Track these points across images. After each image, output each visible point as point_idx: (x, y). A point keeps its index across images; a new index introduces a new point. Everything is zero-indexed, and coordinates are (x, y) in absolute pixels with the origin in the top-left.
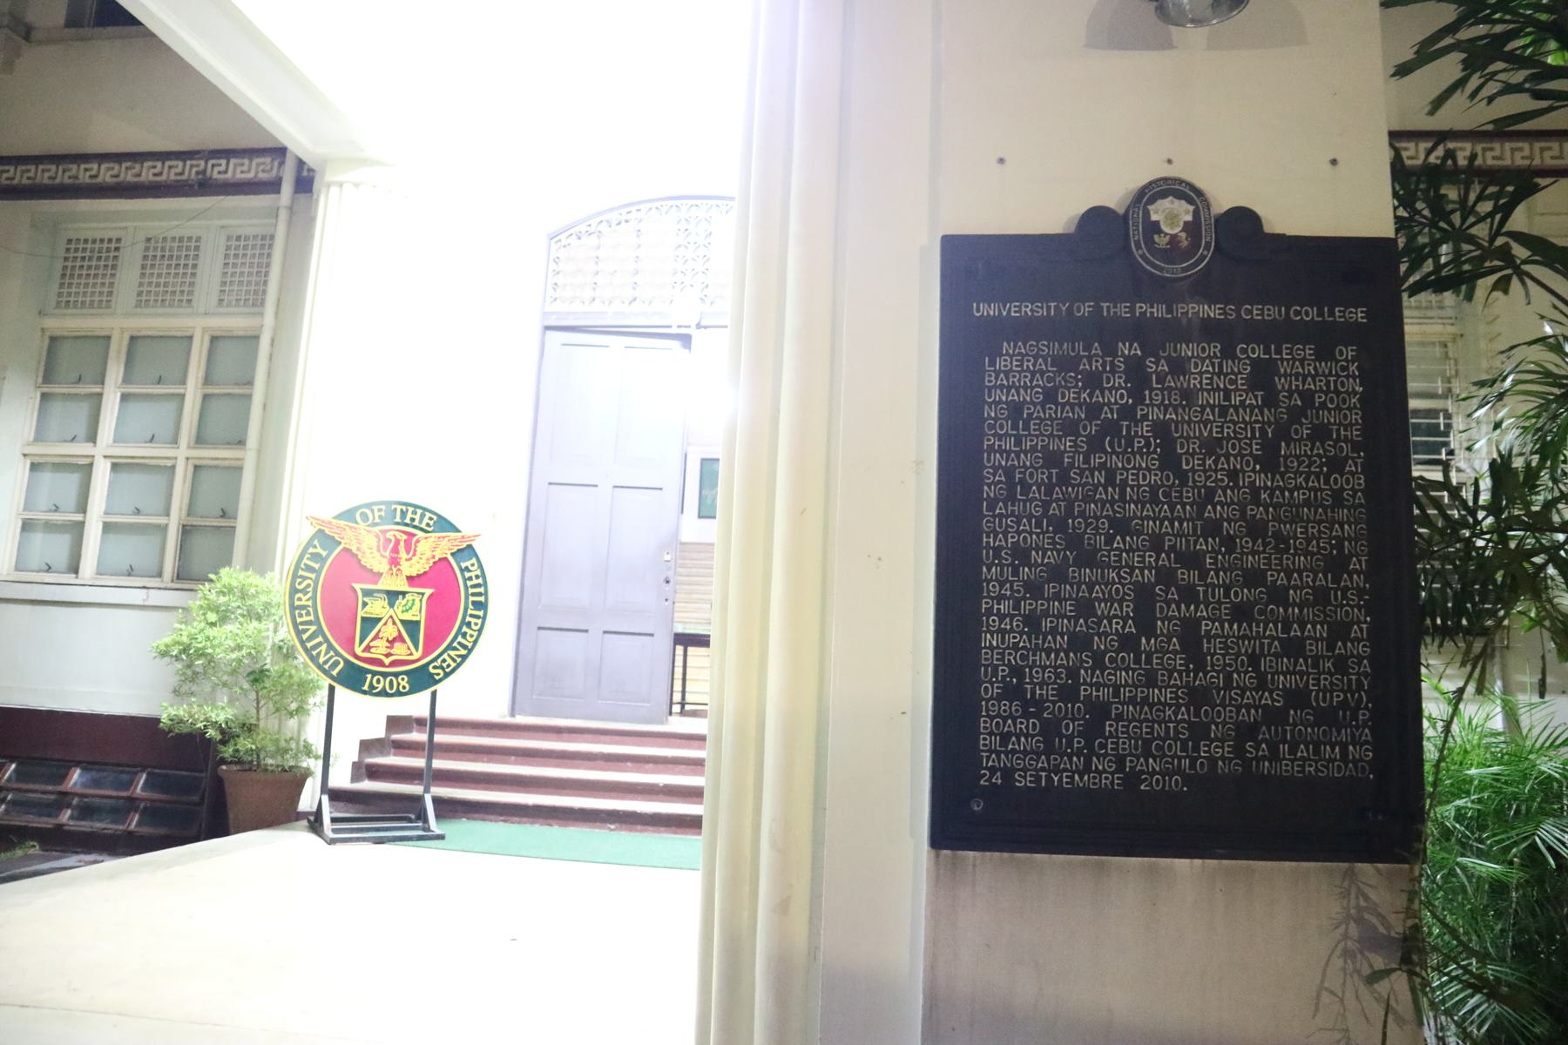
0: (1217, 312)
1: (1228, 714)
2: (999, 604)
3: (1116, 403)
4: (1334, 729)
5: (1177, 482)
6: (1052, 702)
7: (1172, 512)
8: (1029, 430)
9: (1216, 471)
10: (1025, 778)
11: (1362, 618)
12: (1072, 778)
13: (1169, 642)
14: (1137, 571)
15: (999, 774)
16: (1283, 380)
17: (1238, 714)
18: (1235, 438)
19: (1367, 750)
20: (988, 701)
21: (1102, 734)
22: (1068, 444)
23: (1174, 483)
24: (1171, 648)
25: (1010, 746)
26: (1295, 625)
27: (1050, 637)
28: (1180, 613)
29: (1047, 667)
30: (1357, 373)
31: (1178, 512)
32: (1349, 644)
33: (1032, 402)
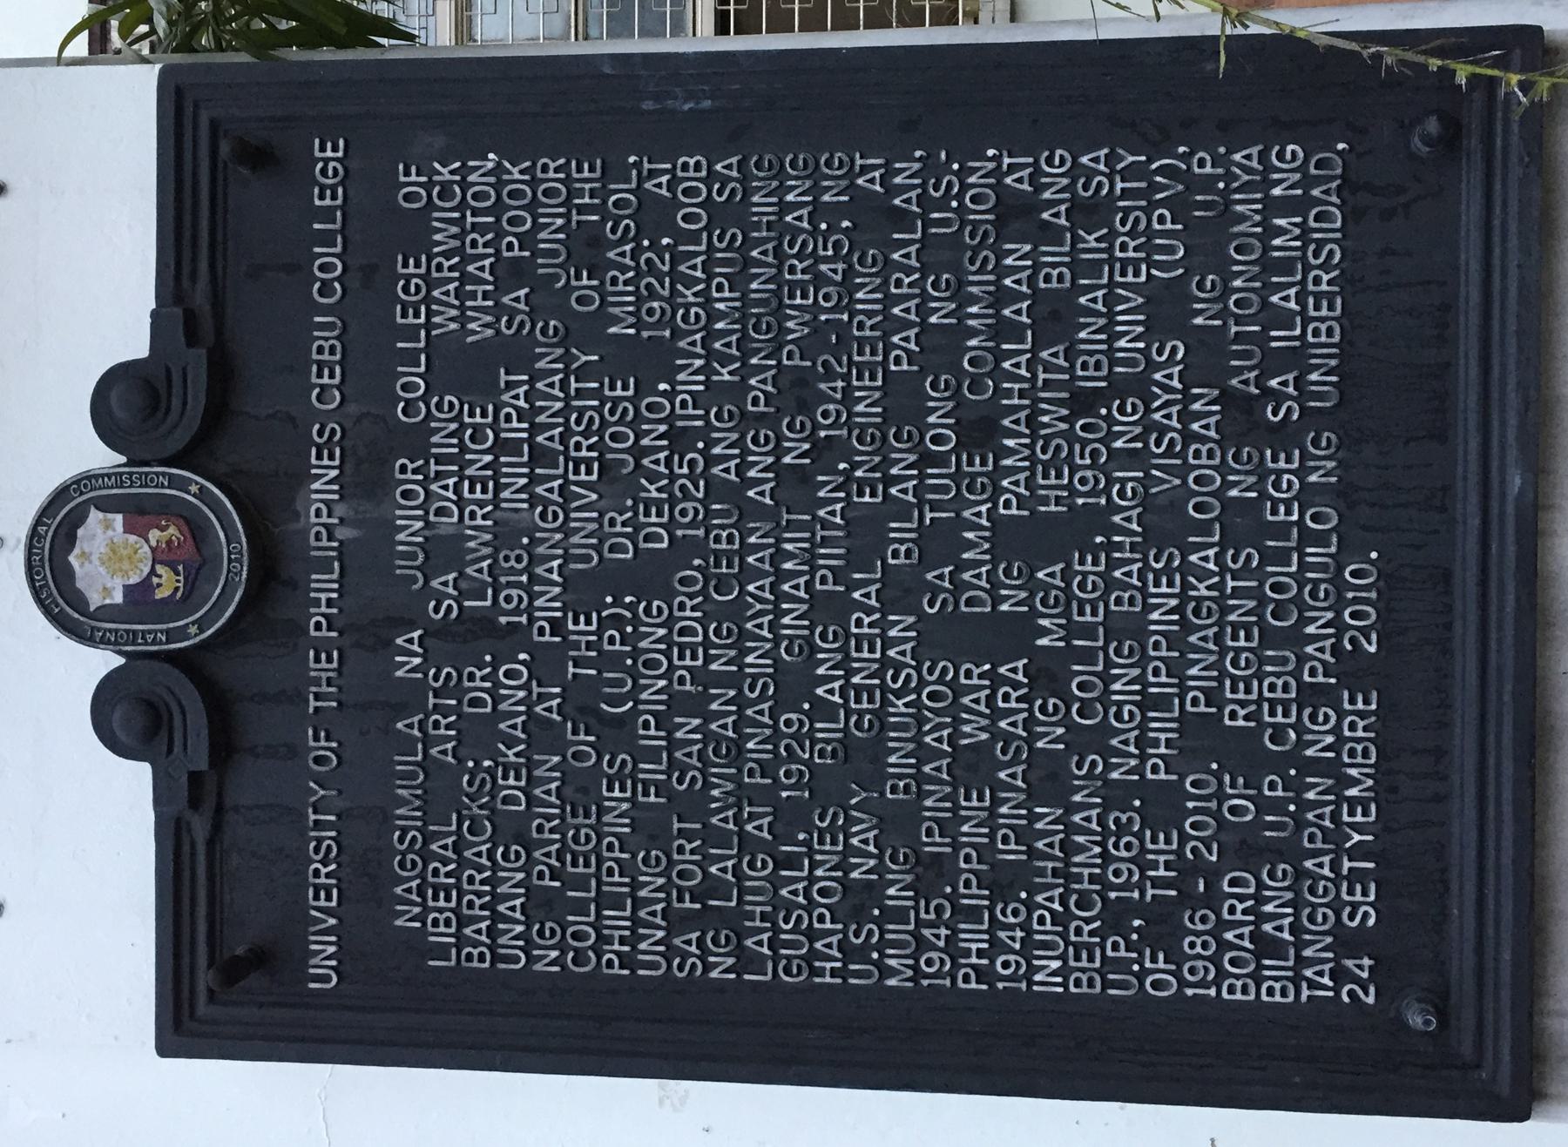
0: (326, 462)
1: (1204, 461)
2: (967, 953)
3: (526, 687)
4: (1236, 229)
5: (697, 562)
6: (1181, 844)
7: (764, 574)
8: (587, 877)
9: (673, 477)
10: (1355, 906)
11: (991, 165)
12: (1352, 802)
13: (1047, 588)
14: (892, 653)
15: (1349, 963)
16: (472, 326)
17: (1203, 439)
18: (600, 432)
19: (1280, 156)
20: (1183, 983)
21: (1254, 735)
22: (617, 794)
23: (698, 568)
24: (1058, 582)
25: (1286, 936)
26: (1006, 312)
27: (1040, 845)
28: (983, 563)
29: (1105, 851)
30: (457, 164)
31: (760, 560)
32: (1047, 195)
33: (525, 869)
